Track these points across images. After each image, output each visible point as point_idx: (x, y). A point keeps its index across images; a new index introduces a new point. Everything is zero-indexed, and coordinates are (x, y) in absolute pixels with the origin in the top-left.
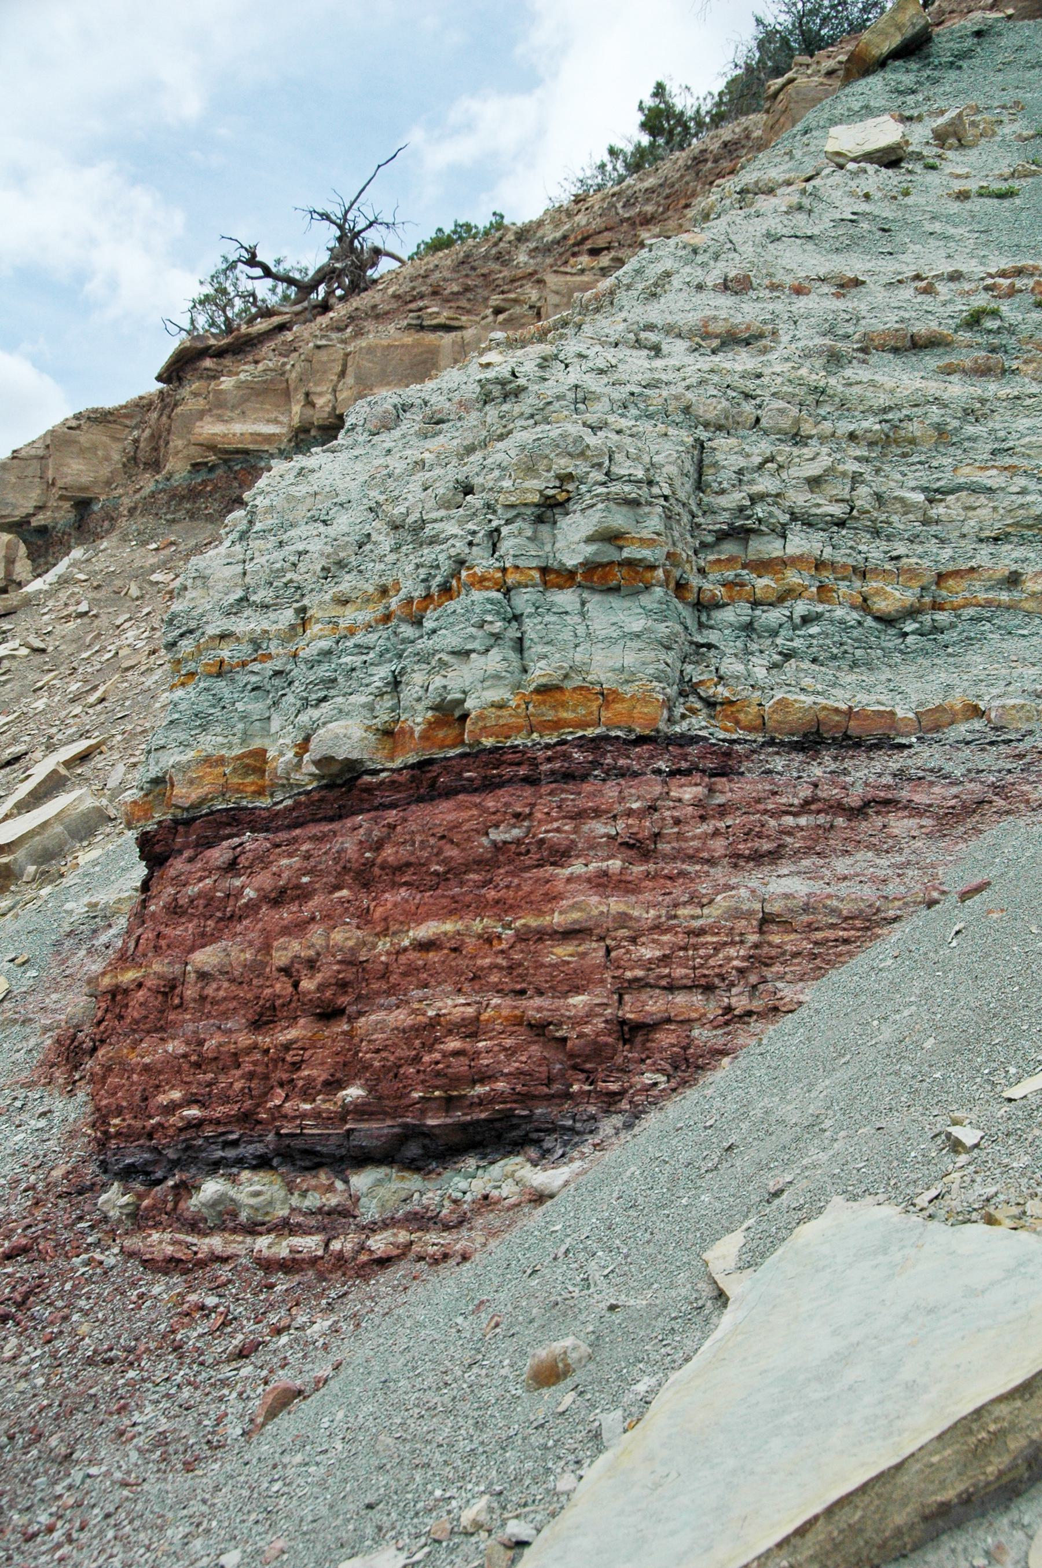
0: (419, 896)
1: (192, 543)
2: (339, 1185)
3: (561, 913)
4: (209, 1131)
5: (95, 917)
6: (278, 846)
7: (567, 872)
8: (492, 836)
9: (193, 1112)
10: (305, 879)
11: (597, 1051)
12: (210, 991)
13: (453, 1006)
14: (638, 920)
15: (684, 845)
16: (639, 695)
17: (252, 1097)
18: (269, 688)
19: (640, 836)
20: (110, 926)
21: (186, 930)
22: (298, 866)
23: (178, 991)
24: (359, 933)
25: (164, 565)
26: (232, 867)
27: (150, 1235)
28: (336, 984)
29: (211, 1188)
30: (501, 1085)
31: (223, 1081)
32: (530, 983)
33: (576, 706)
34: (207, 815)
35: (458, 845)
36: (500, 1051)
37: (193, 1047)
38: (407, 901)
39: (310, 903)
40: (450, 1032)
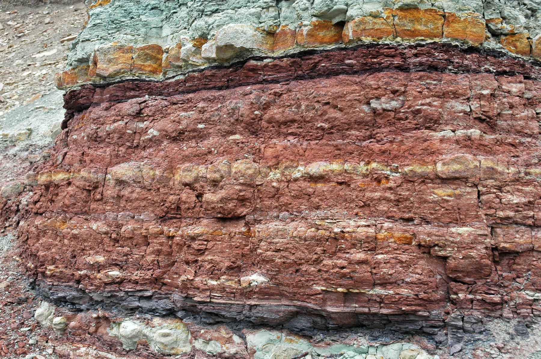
0: (305, 143)
1: (23, 13)
2: (236, 339)
3: (444, 164)
4: (129, 287)
5: (6, 141)
6: (175, 104)
7: (440, 135)
8: (373, 105)
9: (115, 273)
10: (201, 126)
11: (479, 271)
12: (126, 192)
13: (357, 226)
14: (501, 173)
15: (515, 123)
16: (469, 20)
17: (159, 267)
18: (163, 8)
19: (490, 114)
20: (15, 146)
21: (105, 152)
22: (195, 116)
23: (99, 190)
24: (256, 165)
25: (13, 19)
26: (138, 115)
27: (79, 348)
28: (237, 199)
29: (129, 327)
30: (405, 291)
31: (137, 254)
32: (415, 214)
33: (427, 22)
34: (119, 82)
35: (341, 110)
36: (396, 263)
37: (112, 228)
38: (295, 146)
39: (206, 142)
40: (354, 245)
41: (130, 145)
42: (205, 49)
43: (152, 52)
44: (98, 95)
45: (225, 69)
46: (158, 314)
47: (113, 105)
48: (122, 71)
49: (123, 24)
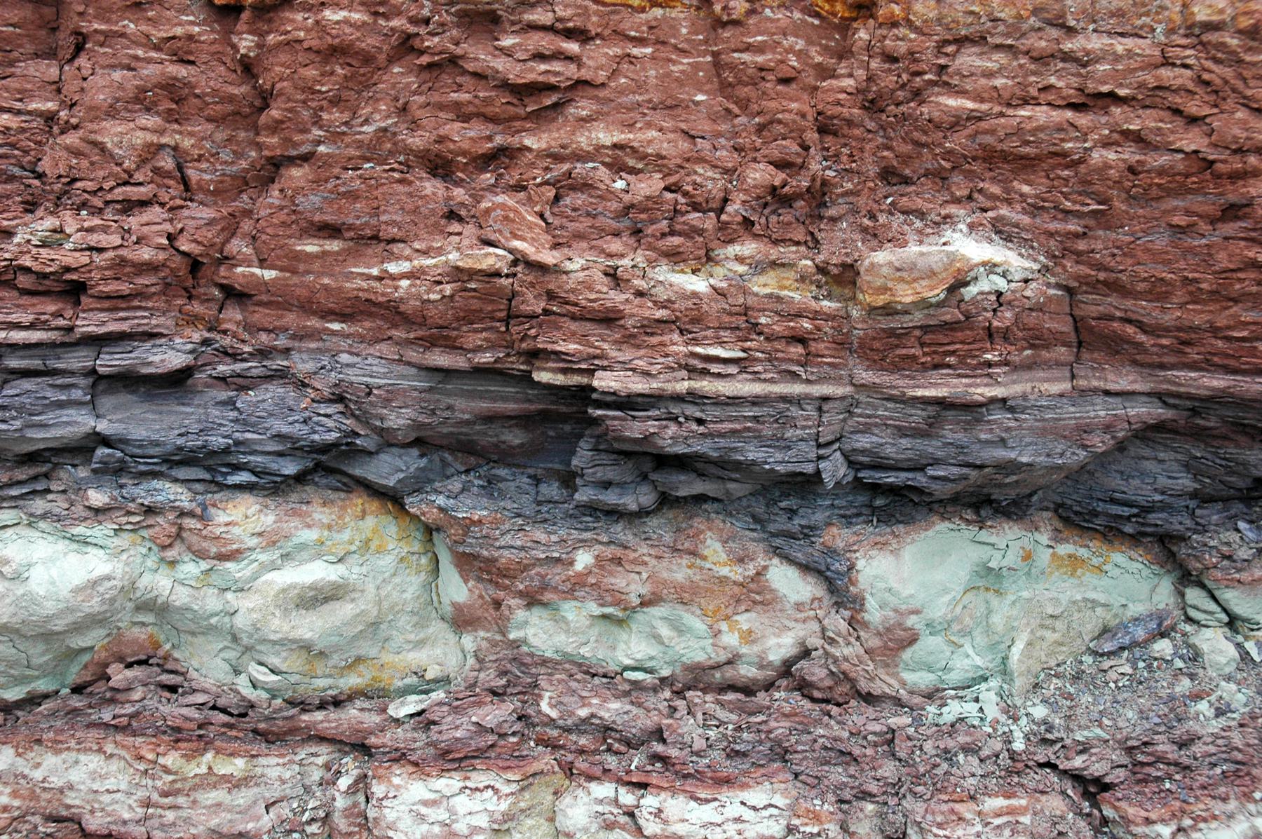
2: (786, 581)
46: (243, 477)
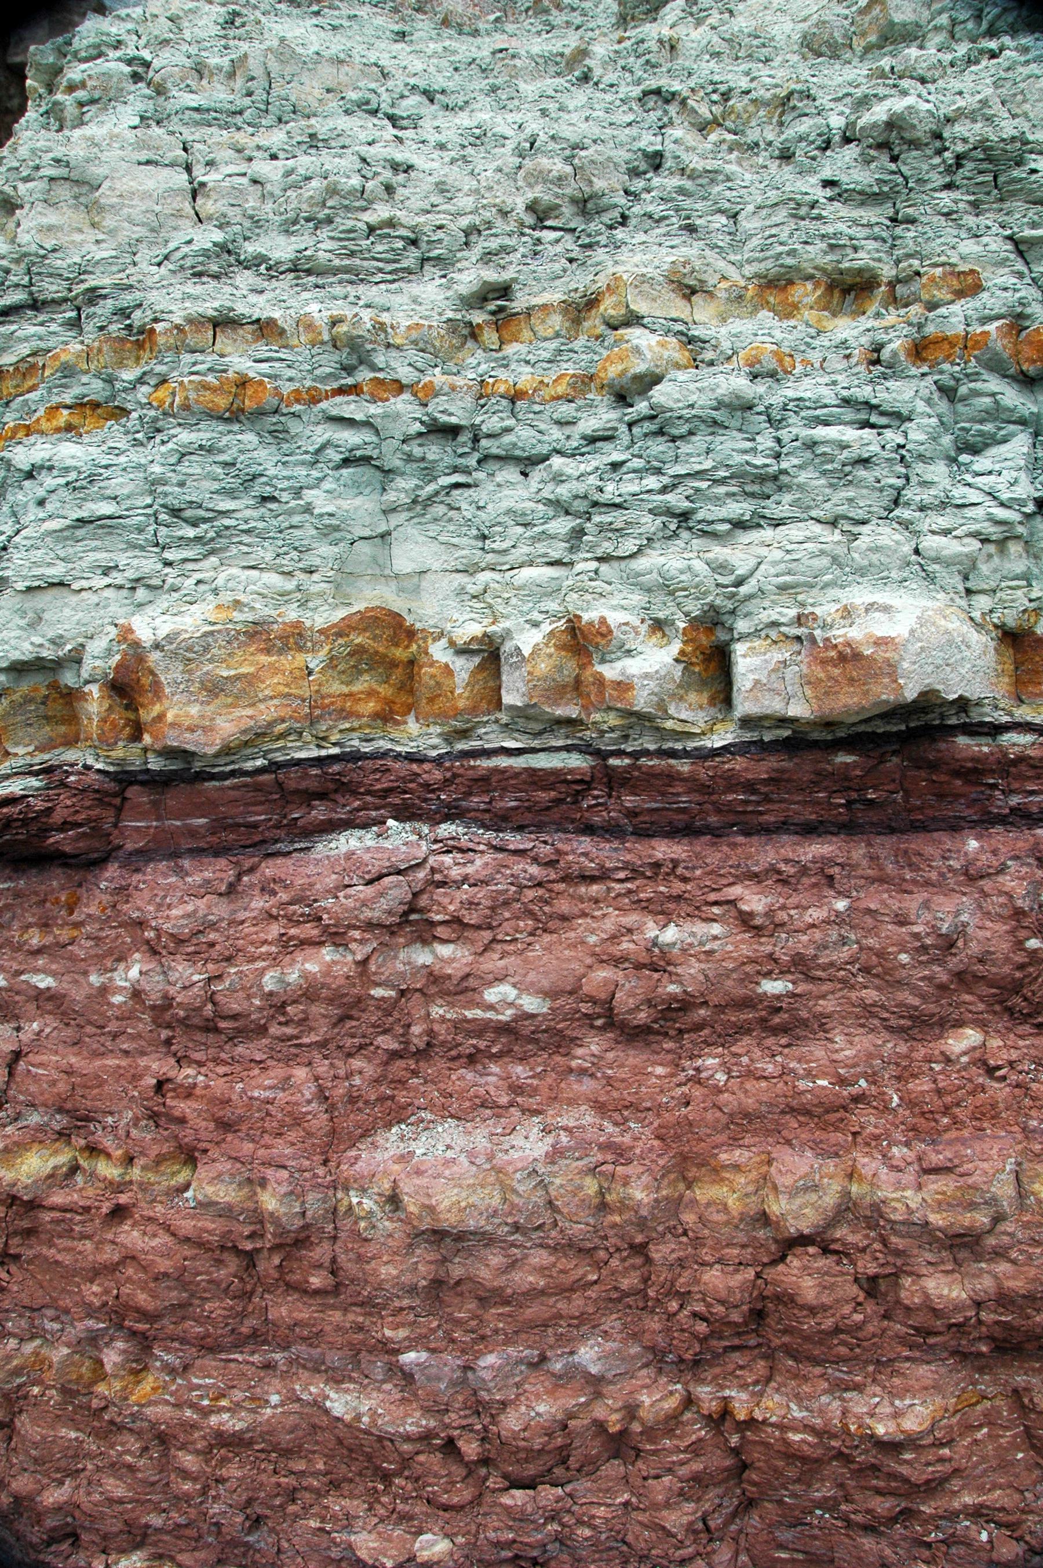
10: (773, 987)
18: (395, 462)
41: (395, 1046)
42: (757, 682)
43: (374, 638)
44: (143, 816)
45: (818, 755)
47: (252, 870)
48: (280, 728)
49: (227, 522)
